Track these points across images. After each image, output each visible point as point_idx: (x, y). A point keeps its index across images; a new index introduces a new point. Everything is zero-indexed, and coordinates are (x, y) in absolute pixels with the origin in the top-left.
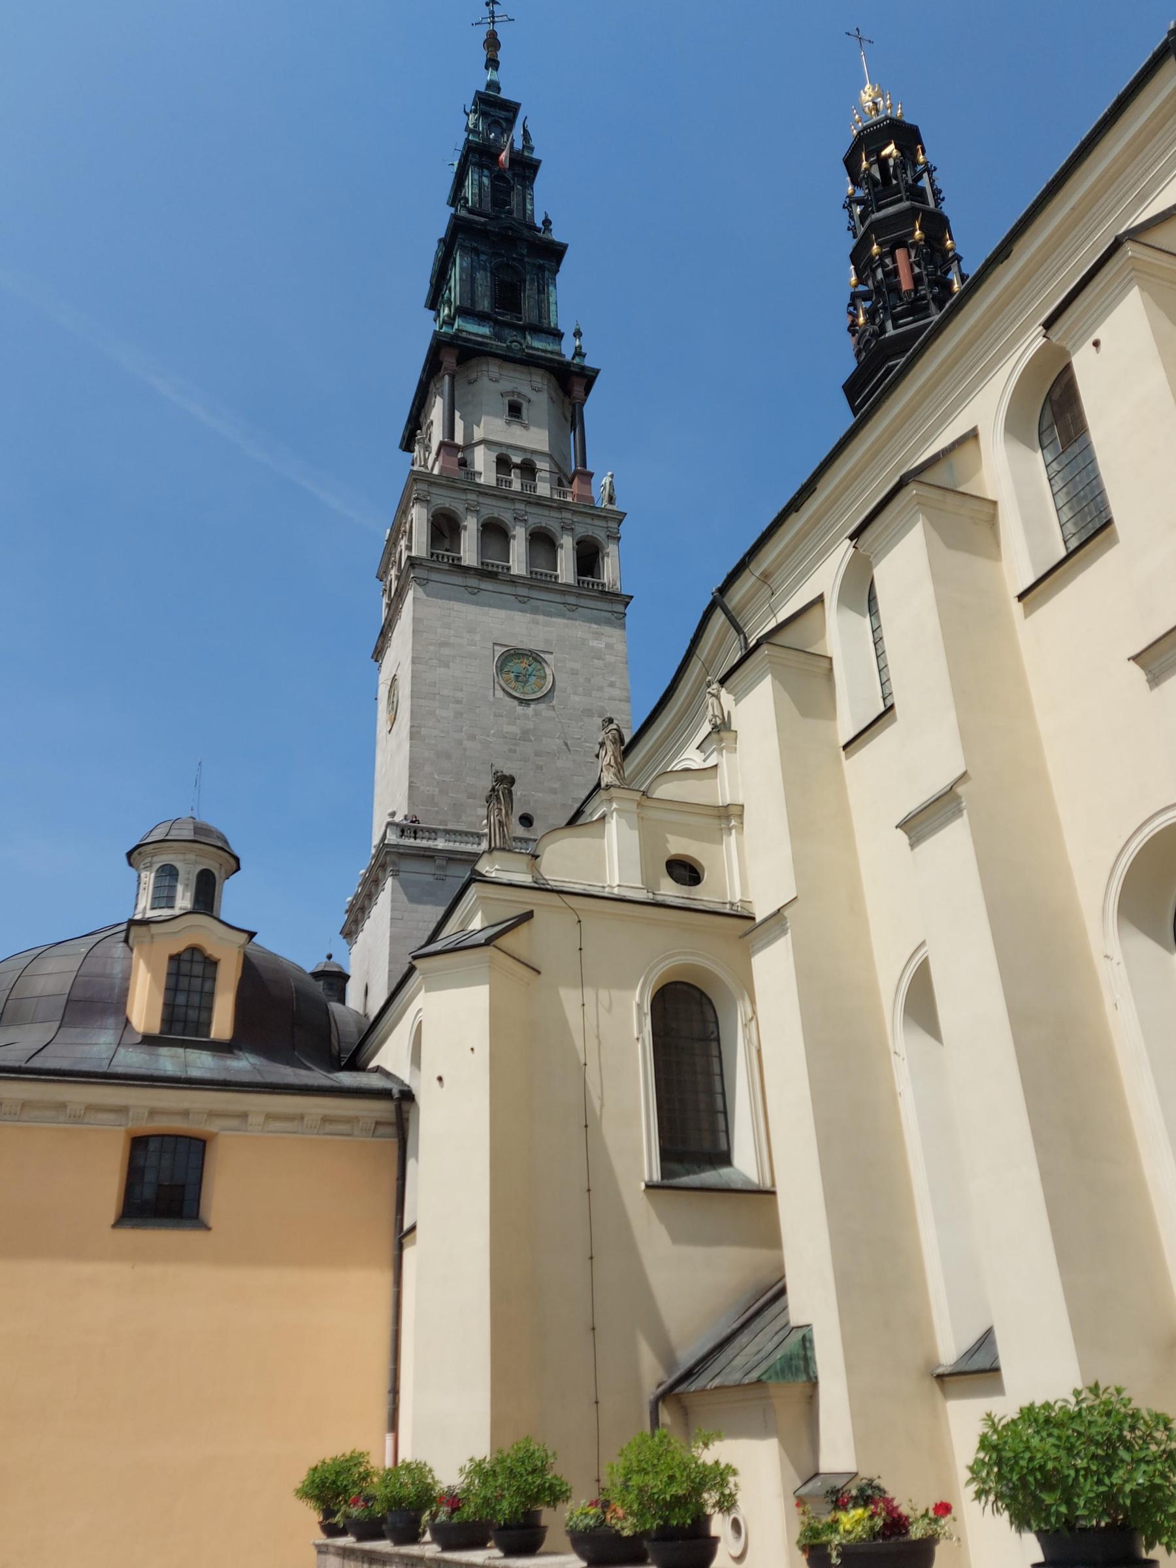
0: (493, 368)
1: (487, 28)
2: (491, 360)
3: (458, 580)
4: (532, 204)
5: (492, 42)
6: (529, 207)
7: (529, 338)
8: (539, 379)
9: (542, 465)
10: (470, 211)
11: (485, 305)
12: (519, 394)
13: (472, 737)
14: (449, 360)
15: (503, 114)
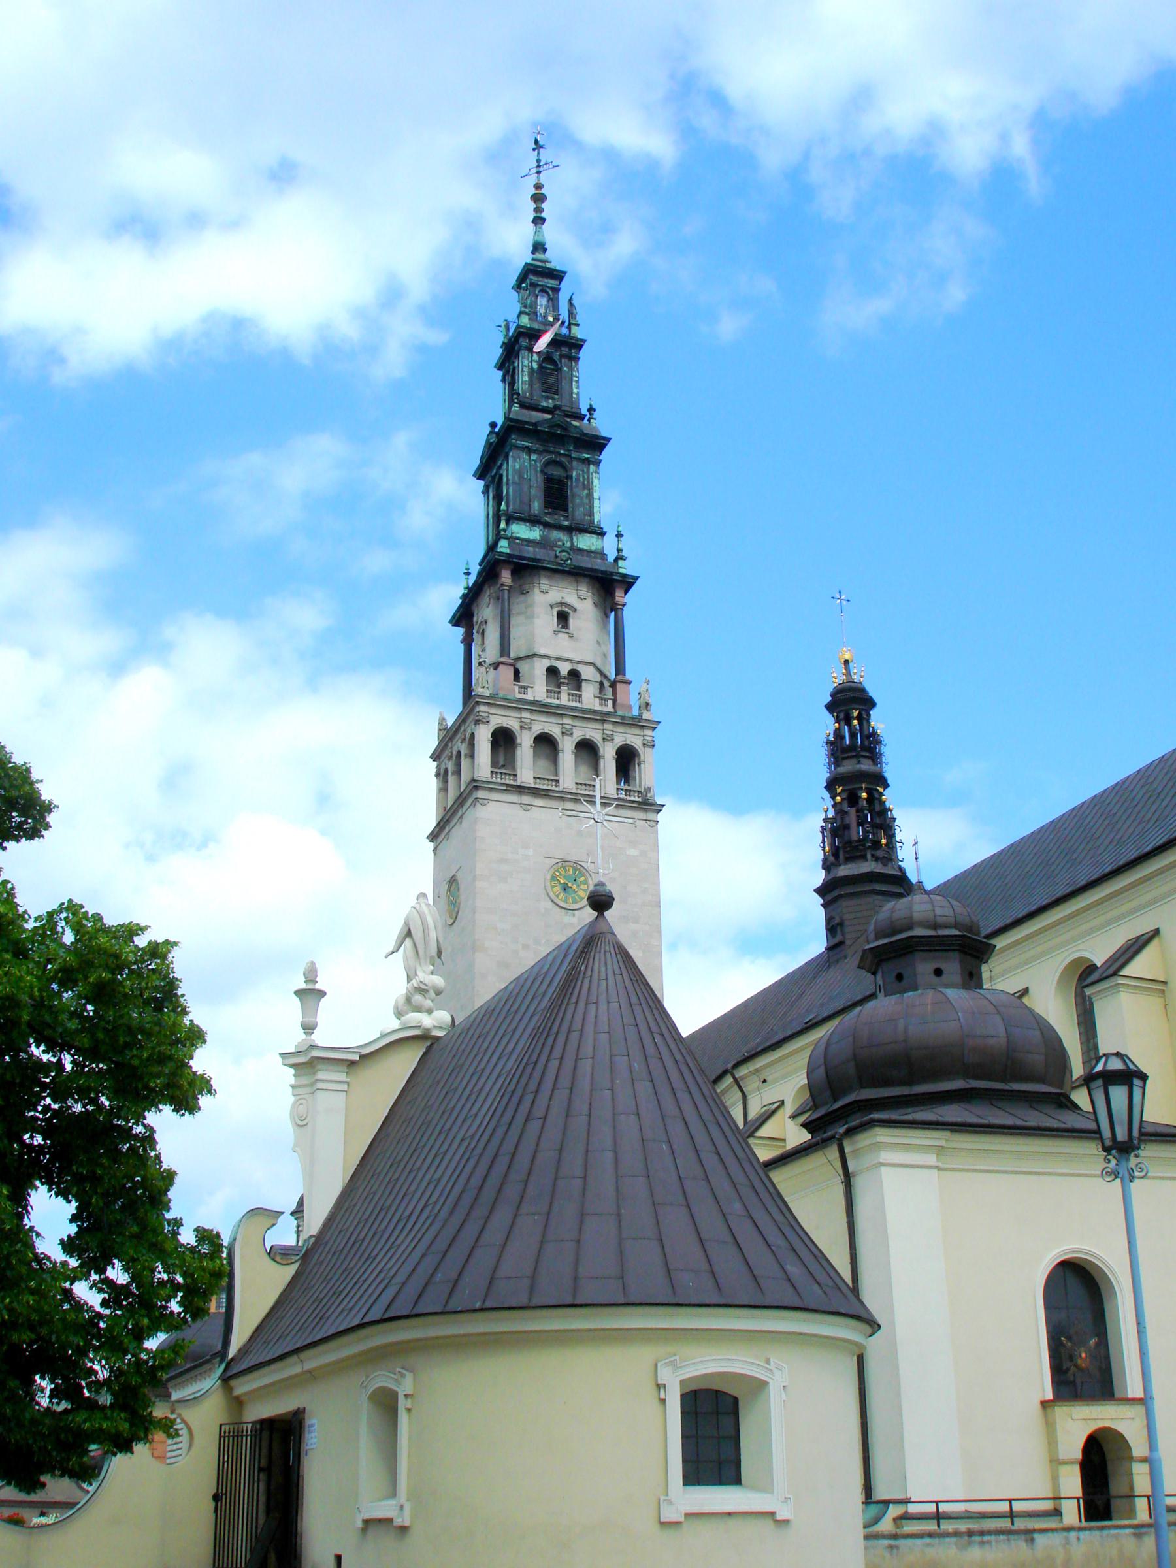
0: (544, 582)
1: (533, 179)
2: (542, 573)
3: (514, 798)
4: (578, 388)
5: (539, 198)
6: (575, 391)
7: (575, 539)
8: (584, 590)
9: (587, 673)
10: (523, 406)
11: (537, 506)
12: (566, 605)
13: (525, 947)
14: (506, 577)
15: (551, 283)
